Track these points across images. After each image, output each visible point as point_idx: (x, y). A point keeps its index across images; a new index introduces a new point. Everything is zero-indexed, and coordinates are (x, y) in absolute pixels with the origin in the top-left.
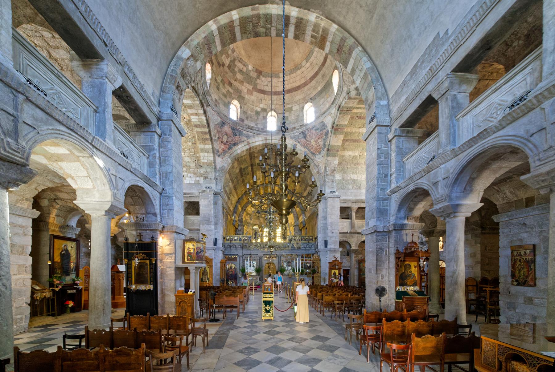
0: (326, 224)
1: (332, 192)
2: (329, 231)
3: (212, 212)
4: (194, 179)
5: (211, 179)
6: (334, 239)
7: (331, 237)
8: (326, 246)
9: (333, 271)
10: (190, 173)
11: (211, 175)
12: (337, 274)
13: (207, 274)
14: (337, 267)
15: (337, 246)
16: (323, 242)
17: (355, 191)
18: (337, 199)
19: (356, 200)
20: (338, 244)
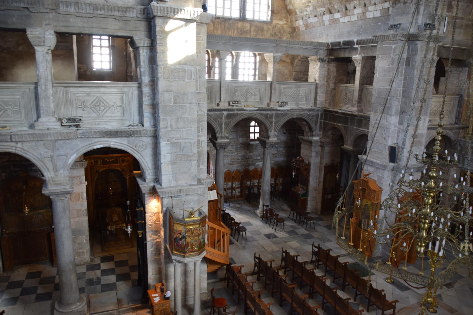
4: (379, 7)
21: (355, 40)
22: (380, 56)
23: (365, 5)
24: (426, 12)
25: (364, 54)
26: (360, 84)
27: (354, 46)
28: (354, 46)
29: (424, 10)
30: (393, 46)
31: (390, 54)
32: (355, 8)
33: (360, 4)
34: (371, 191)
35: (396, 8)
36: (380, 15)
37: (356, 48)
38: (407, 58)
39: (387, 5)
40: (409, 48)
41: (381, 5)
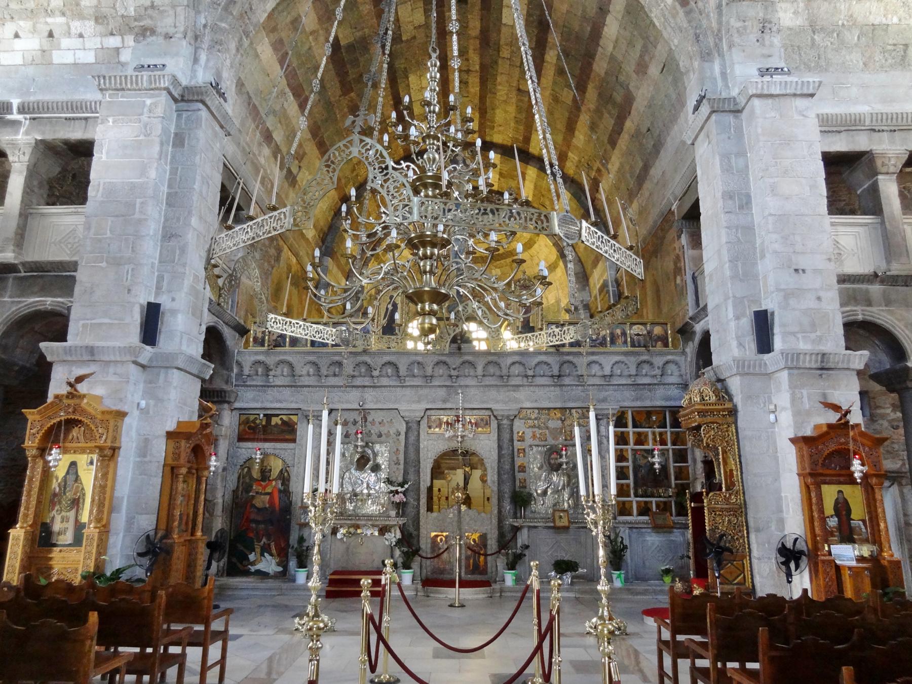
0: (749, 229)
1: (765, 72)
2: (767, 267)
3: (153, 174)
4: (96, 43)
5: (168, 37)
6: (809, 302)
7: (788, 295)
8: (764, 344)
9: (830, 493)
10: (81, 17)
11: (169, 21)
12: (858, 511)
13: (76, 503)
14: (857, 468)
15: (834, 340)
16: (747, 323)
17: (882, 77)
18: (800, 103)
19: (892, 117)
20: (840, 331)
21: (15, 102)
22: (111, 120)
23: (51, 35)
24: (211, 64)
25: (43, 133)
26: (22, 202)
27: (9, 117)
28: (9, 117)
29: (208, 60)
30: (148, 102)
31: (142, 114)
32: (17, 36)
33: (34, 30)
34: (92, 418)
35: (145, 42)
36: (94, 61)
37: (15, 124)
38: (176, 134)
39: (114, 42)
40: (179, 116)
41: (98, 39)
